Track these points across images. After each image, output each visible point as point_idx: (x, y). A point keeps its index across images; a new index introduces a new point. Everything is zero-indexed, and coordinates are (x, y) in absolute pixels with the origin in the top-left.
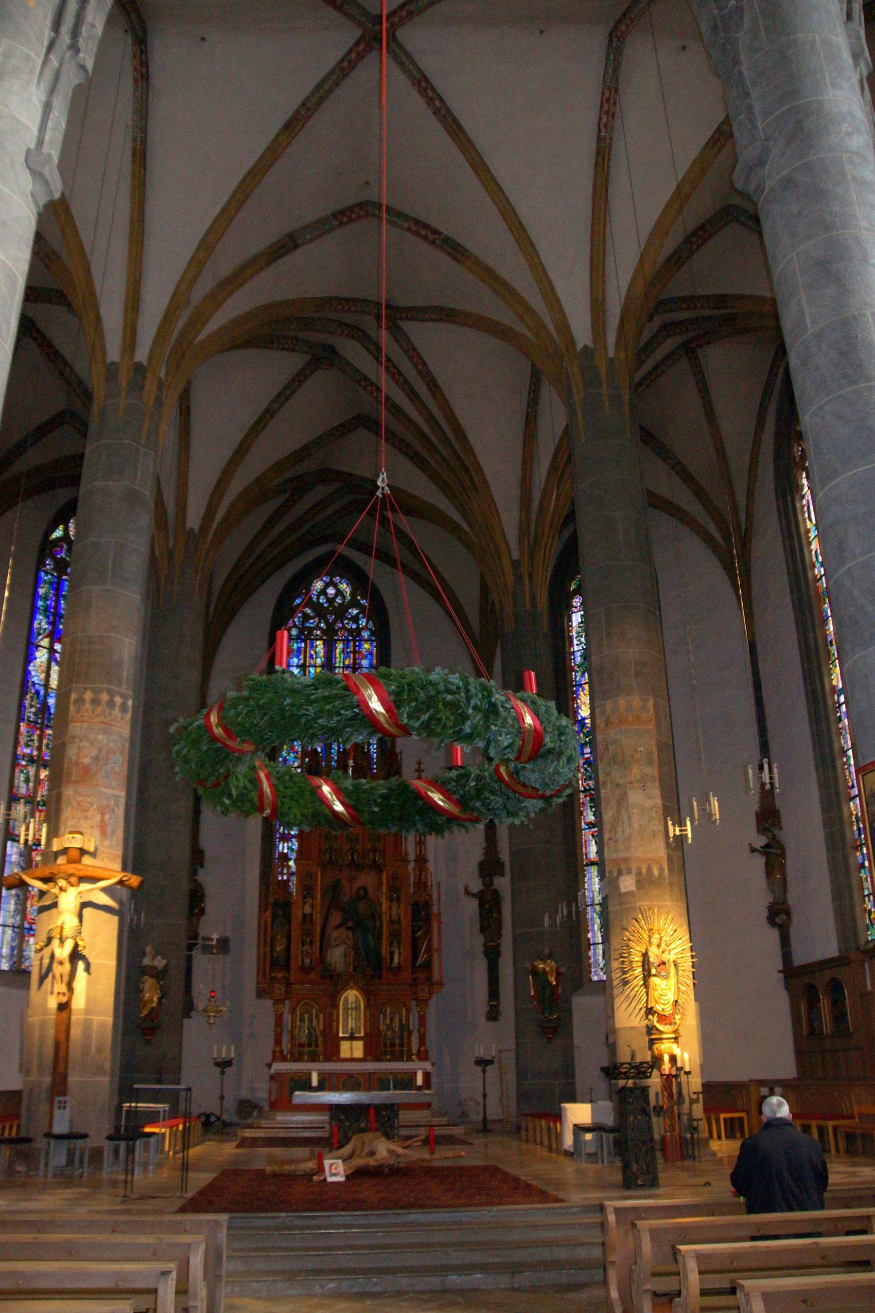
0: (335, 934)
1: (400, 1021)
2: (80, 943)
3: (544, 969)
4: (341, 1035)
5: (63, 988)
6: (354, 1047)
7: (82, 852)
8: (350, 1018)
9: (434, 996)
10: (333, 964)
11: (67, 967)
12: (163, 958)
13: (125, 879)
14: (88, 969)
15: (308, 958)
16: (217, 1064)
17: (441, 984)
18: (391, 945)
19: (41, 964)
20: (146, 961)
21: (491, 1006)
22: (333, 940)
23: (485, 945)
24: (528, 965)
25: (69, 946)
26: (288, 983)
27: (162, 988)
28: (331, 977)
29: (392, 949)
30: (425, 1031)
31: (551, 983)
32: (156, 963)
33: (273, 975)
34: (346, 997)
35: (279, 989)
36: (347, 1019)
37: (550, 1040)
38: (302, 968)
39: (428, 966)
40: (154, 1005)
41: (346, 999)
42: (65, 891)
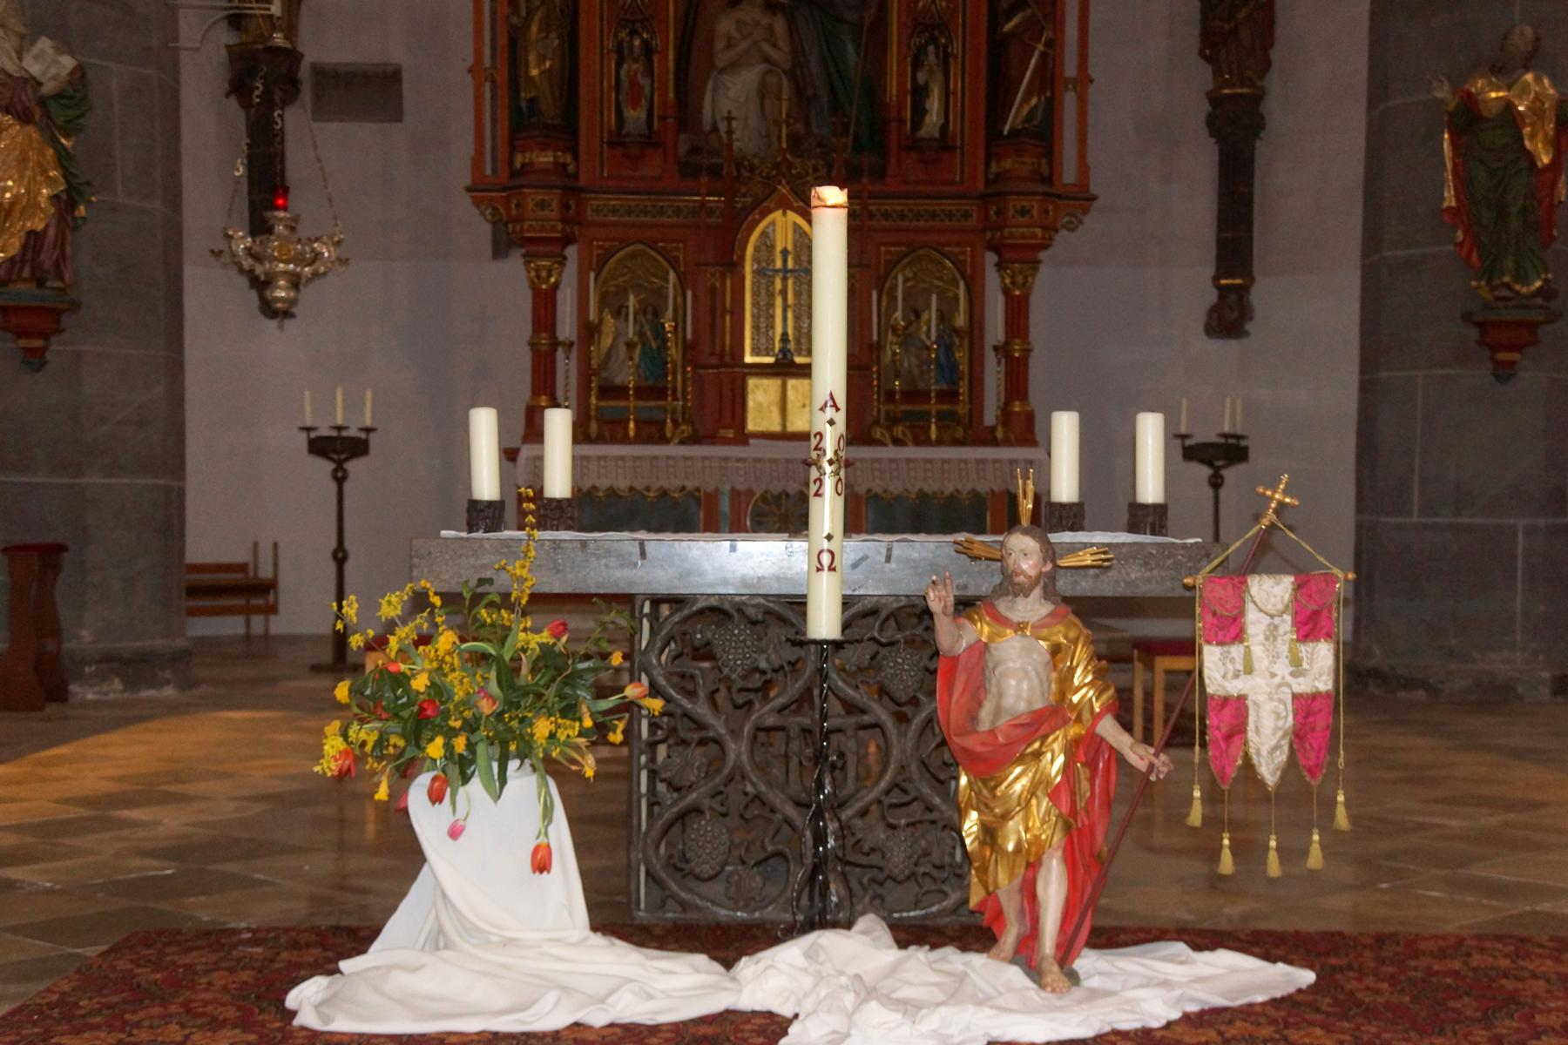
0: (726, 25)
1: (943, 317)
3: (1509, 107)
4: (749, 359)
6: (791, 394)
8: (779, 301)
9: (1063, 237)
10: (723, 127)
12: (64, 46)
15: (635, 105)
16: (320, 447)
17: (1082, 198)
18: (917, 65)
21: (1221, 288)
22: (720, 44)
23: (1215, 99)
24: (1443, 92)
26: (572, 191)
27: (64, 160)
28: (715, 172)
29: (922, 78)
30: (1027, 352)
31: (1531, 157)
32: (35, 69)
33: (519, 160)
34: (764, 234)
35: (540, 207)
36: (771, 305)
37: (1504, 371)
38: (618, 140)
39: (1043, 135)
40: (40, 226)
41: (767, 244)
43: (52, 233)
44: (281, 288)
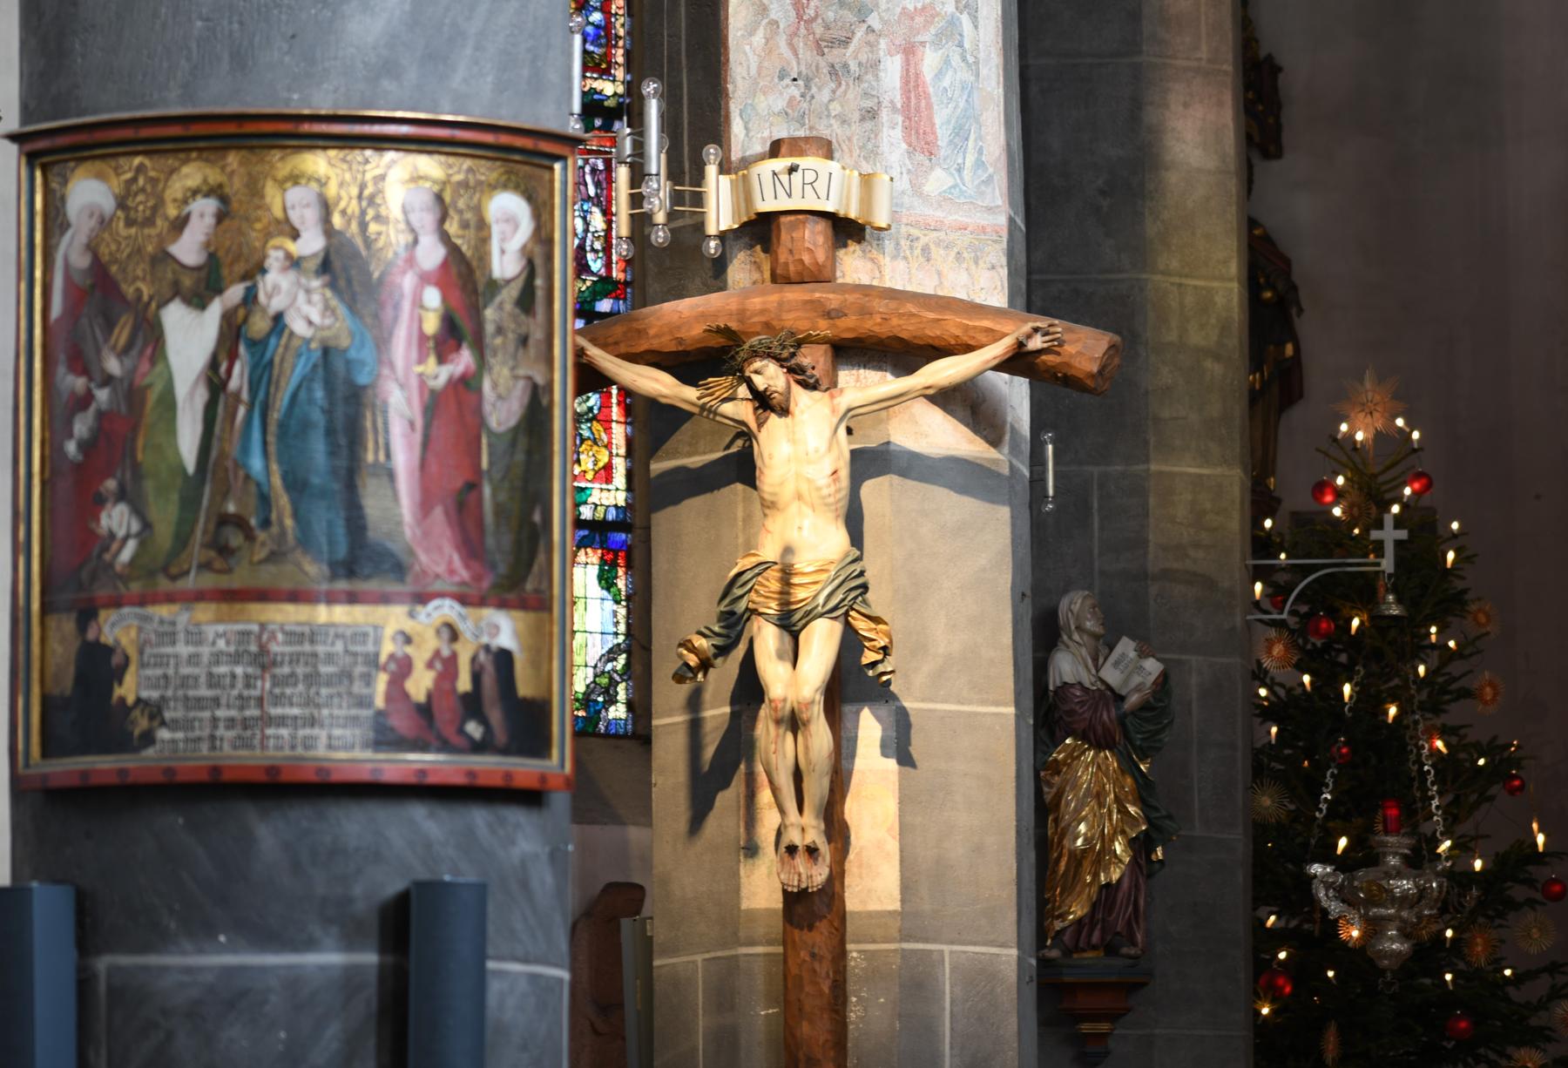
2: (861, 625)
5: (808, 829)
7: (845, 230)
11: (820, 735)
13: (1036, 343)
14: (900, 747)
19: (695, 726)
20: (1067, 667)
25: (821, 642)
27: (1145, 791)
32: (1111, 675)
42: (784, 411)
43: (1125, 884)
44: (1392, 940)
